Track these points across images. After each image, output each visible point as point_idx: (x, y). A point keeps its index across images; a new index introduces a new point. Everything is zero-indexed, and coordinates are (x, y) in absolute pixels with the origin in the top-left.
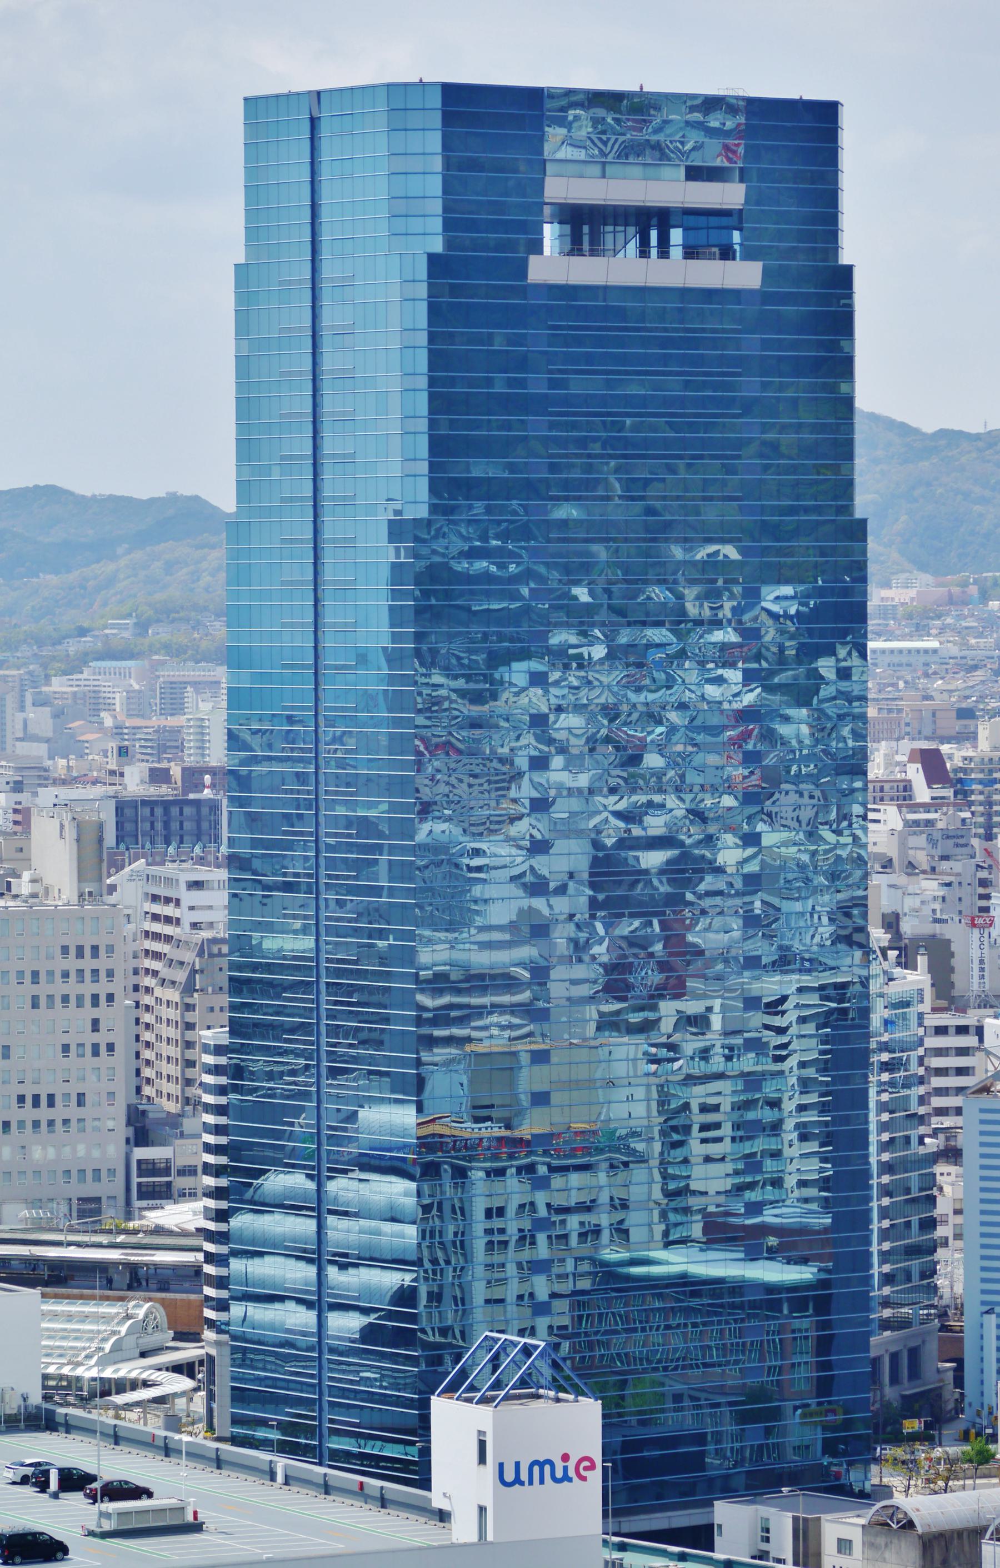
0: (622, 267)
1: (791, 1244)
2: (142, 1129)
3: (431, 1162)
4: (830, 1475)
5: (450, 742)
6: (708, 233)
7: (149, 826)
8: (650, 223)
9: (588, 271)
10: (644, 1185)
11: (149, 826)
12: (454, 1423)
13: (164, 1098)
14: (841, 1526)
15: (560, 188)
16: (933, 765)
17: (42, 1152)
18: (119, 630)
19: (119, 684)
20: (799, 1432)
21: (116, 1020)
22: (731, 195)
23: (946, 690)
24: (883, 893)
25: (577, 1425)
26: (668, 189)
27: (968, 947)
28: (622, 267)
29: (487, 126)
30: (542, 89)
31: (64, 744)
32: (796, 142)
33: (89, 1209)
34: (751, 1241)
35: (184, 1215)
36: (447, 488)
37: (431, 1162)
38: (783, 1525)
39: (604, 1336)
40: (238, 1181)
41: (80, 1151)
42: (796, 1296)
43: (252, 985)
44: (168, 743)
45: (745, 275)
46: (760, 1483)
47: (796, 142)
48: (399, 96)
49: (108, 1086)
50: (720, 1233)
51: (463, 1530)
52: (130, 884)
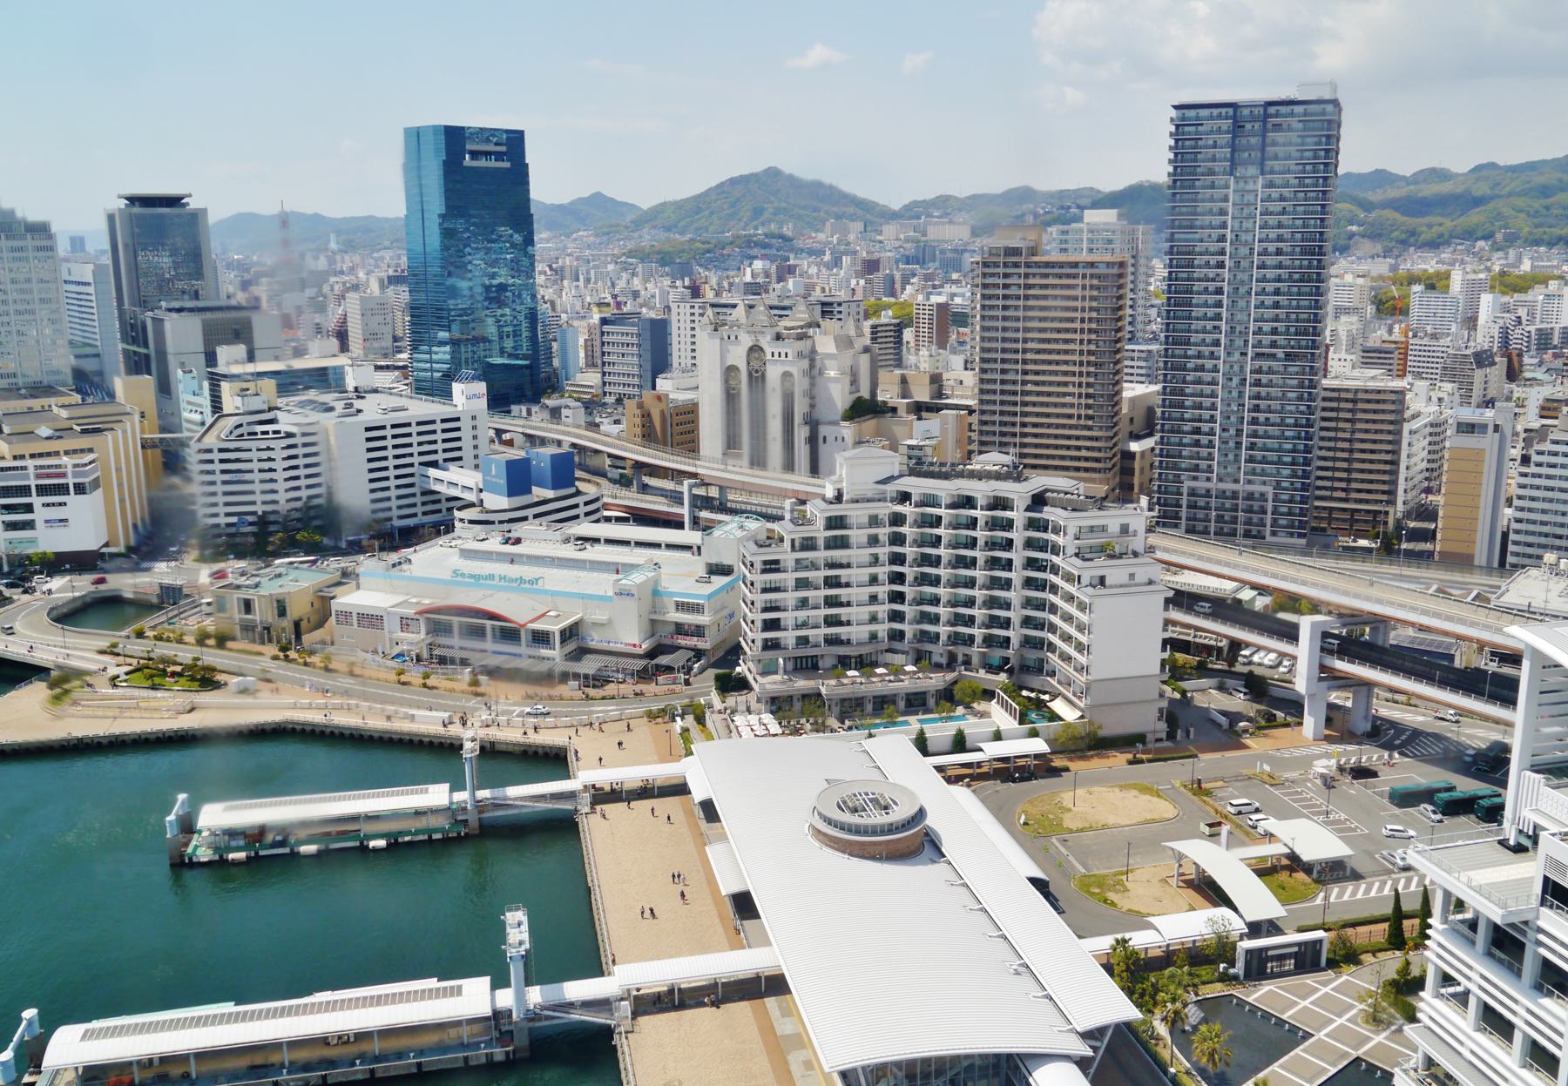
0: (482, 163)
1: (525, 357)
2: (395, 339)
3: (454, 343)
4: (535, 399)
5: (453, 259)
6: (499, 156)
7: (394, 280)
8: (487, 154)
9: (475, 164)
10: (496, 346)
11: (394, 280)
12: (457, 388)
13: (399, 333)
14: (535, 409)
15: (469, 147)
16: (550, 267)
17: (376, 345)
18: (387, 243)
19: (387, 254)
20: (529, 393)
21: (389, 318)
22: (504, 149)
23: (553, 254)
24: (541, 291)
25: (481, 387)
26: (491, 148)
27: (558, 302)
28: (482, 163)
29: (454, 137)
30: (463, 128)
31: (377, 266)
32: (515, 141)
33: (385, 356)
34: (517, 357)
35: (404, 356)
36: (447, 207)
37: (454, 343)
38: (524, 408)
39: (487, 373)
40: (415, 349)
41: (384, 344)
42: (526, 367)
43: (415, 310)
44: (398, 265)
45: (507, 165)
46: (519, 402)
47: (515, 141)
48: (436, 128)
49: (388, 329)
50: (510, 356)
51: (460, 408)
52: (391, 290)
